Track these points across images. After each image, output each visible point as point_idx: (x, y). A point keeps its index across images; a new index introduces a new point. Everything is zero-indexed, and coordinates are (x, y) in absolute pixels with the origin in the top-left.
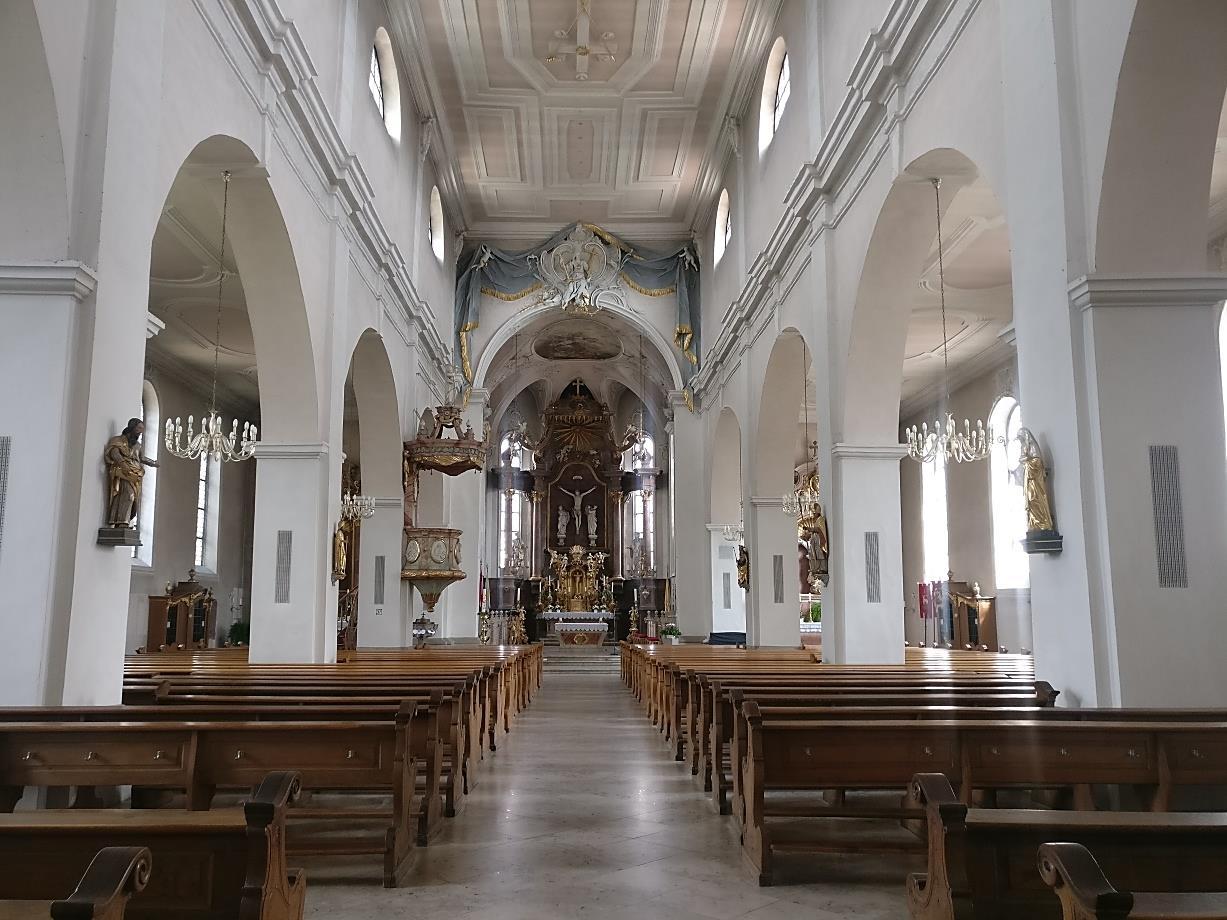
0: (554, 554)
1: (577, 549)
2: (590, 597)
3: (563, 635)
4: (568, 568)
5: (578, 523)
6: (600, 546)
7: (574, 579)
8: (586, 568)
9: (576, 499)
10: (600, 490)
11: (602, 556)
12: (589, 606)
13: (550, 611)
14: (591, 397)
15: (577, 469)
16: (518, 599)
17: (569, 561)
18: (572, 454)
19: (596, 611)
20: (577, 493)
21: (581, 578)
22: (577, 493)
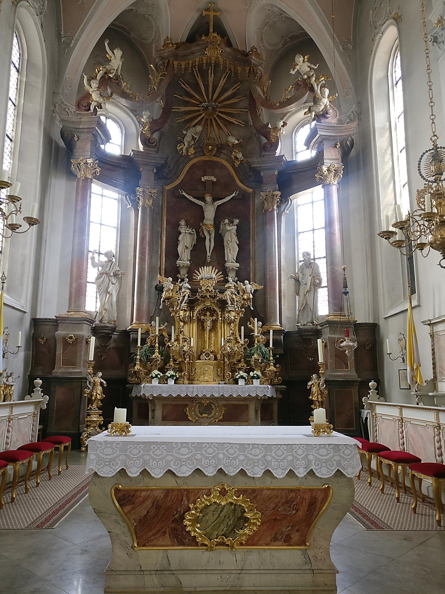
0: (168, 283)
1: (208, 274)
2: (229, 356)
3: (126, 498)
4: (192, 304)
5: (209, 244)
6: (242, 276)
7: (201, 324)
8: (223, 304)
10: (244, 198)
11: (249, 287)
12: (228, 373)
13: (155, 382)
14: (229, 44)
15: (208, 167)
16: (91, 358)
17: (193, 291)
18: (200, 146)
19: (241, 382)
20: (209, 199)
21: (214, 322)
22: (209, 199)
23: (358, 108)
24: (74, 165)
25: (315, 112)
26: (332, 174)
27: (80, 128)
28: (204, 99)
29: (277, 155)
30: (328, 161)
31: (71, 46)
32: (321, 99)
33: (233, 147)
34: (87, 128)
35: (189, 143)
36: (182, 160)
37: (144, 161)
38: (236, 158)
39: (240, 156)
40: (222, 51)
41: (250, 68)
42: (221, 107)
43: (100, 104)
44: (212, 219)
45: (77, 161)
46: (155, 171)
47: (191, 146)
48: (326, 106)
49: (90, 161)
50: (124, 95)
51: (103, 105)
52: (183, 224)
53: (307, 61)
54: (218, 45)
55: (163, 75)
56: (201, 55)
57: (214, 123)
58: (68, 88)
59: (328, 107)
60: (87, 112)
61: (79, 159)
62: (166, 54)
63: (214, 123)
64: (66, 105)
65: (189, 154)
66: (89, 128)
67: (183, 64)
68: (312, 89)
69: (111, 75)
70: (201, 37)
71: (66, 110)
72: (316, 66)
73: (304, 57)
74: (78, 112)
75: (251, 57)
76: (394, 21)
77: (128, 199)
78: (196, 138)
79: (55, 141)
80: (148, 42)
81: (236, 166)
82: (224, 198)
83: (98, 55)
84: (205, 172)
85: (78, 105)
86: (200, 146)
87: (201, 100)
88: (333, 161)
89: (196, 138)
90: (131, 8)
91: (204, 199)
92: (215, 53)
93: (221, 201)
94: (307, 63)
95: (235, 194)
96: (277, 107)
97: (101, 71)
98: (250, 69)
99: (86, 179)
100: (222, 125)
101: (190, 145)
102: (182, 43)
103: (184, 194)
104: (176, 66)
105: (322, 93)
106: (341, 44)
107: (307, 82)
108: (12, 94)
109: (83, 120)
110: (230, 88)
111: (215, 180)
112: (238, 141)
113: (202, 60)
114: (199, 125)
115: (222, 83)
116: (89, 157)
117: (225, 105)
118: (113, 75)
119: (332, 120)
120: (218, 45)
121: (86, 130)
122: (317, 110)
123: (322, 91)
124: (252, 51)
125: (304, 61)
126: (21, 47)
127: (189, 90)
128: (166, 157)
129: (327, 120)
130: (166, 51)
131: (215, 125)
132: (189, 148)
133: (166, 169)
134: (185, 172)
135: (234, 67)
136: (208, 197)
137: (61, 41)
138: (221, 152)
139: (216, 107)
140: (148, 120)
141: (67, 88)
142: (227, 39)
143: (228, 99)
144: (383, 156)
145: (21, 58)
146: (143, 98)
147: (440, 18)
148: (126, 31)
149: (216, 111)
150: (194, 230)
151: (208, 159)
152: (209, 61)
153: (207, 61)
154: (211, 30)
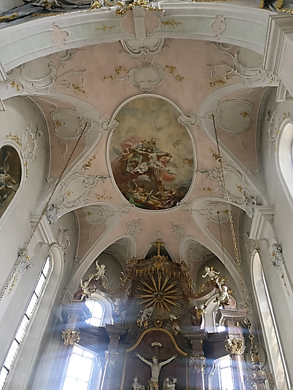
9: (153, 369)
14: (170, 259)
15: (156, 336)
20: (155, 360)
22: (155, 360)
23: (251, 298)
24: (63, 335)
25: (220, 301)
26: (236, 346)
27: (72, 311)
28: (156, 291)
29: (201, 328)
30: (232, 336)
31: (80, 263)
32: (223, 293)
33: (173, 321)
34: (76, 311)
35: (144, 318)
36: (139, 330)
37: (113, 331)
38: (175, 328)
39: (178, 328)
40: (163, 264)
41: (181, 273)
42: (165, 295)
43: (88, 295)
44: (157, 377)
45: (66, 332)
46: (119, 338)
47: (146, 321)
48: (226, 297)
49: (73, 332)
50: (103, 290)
51: (89, 296)
52: (136, 381)
53: (213, 270)
54: (161, 261)
55: (128, 278)
56: (151, 266)
57: (162, 305)
58: (74, 285)
59: (228, 297)
60: (78, 300)
61: (67, 331)
62: (131, 266)
63: (162, 305)
64: (70, 295)
65: (144, 326)
66: (77, 310)
67: (141, 271)
68: (217, 287)
69: (96, 279)
70: (153, 256)
71: (70, 298)
72: (218, 273)
73: (210, 268)
74: (74, 300)
75: (181, 267)
76: (256, 250)
77: (99, 359)
78: (149, 316)
79: (58, 318)
80: (124, 258)
81: (176, 335)
82: (167, 360)
83: (93, 269)
84: (154, 339)
85: (75, 296)
86: (151, 321)
87: (154, 291)
88: (235, 336)
89: (149, 316)
90: (116, 243)
91: (152, 360)
92: (160, 264)
93: (164, 362)
94: (212, 271)
95: (175, 357)
96: (196, 297)
97: (92, 277)
98: (181, 274)
99: (69, 345)
100: (166, 306)
101: (145, 320)
102: (142, 260)
103: (139, 356)
104: (137, 272)
105: (223, 289)
106: (234, 260)
107: (214, 282)
108: (38, 290)
109: (75, 305)
110: (172, 284)
111: (161, 345)
112: (177, 317)
113: (152, 269)
114: (151, 307)
115: (166, 281)
116: (74, 329)
117: (169, 294)
118: (98, 278)
119: (232, 306)
120: (161, 261)
121: (75, 312)
122: (221, 300)
123: (223, 288)
124: (182, 263)
125: (210, 270)
126: (50, 265)
127: (147, 285)
128: (127, 328)
129: (228, 306)
130: (132, 264)
131: (162, 307)
132: (145, 322)
133: (127, 337)
134: (141, 339)
135: (171, 272)
136: (155, 359)
137: (75, 261)
138: (166, 325)
139: (163, 295)
140: (118, 304)
141: (73, 285)
142: (168, 257)
143: (170, 290)
144: (270, 334)
145: (49, 271)
146: (114, 291)
147: (273, 253)
148: (113, 253)
149: (163, 298)
150: (143, 386)
151: (157, 330)
152: (155, 270)
153: (155, 269)
154: (159, 253)
